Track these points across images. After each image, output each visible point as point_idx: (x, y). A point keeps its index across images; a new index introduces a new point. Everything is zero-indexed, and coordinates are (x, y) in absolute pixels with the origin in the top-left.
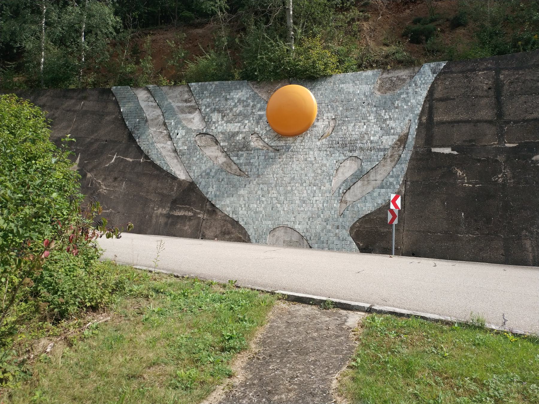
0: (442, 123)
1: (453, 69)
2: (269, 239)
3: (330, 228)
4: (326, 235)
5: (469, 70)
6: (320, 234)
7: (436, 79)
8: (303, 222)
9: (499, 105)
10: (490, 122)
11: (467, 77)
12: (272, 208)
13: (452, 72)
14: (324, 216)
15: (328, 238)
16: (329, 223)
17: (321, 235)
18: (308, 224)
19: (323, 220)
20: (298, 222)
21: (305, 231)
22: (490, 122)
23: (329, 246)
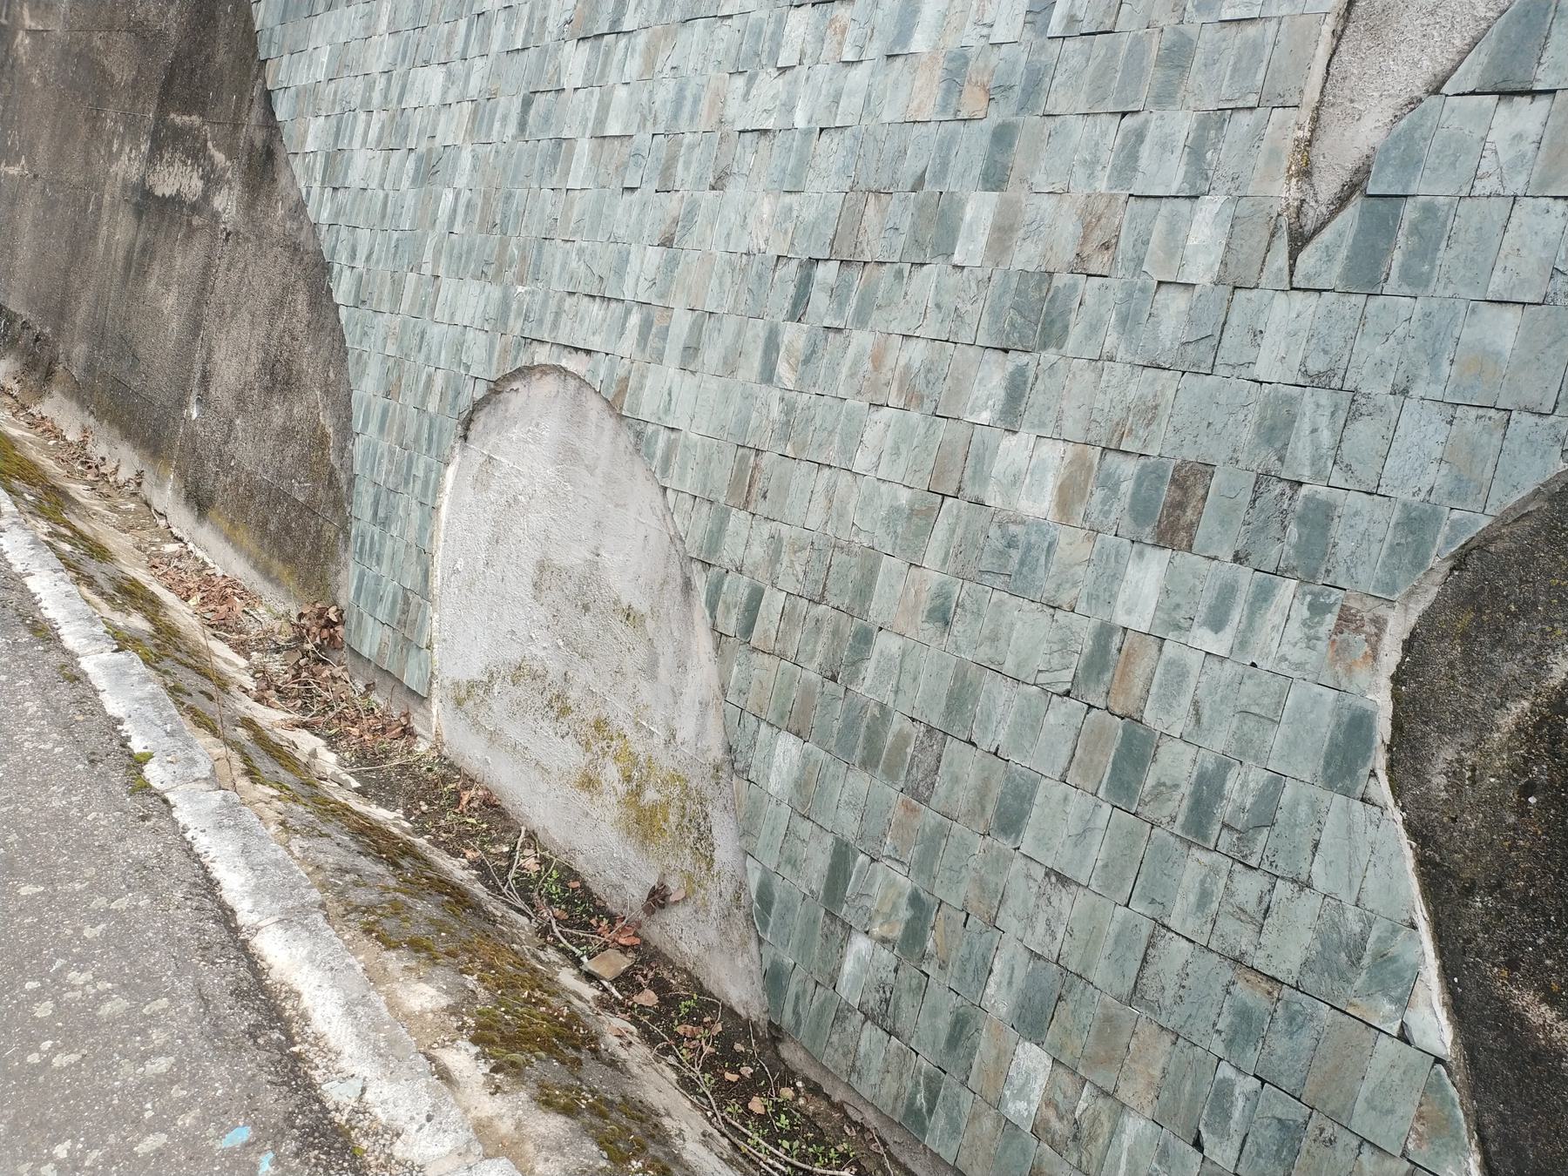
2: (453, 503)
3: (1038, 503)
4: (942, 616)
6: (864, 592)
8: (730, 324)
12: (527, 104)
14: (1003, 234)
15: (960, 698)
16: (1036, 398)
17: (879, 607)
18: (768, 375)
19: (979, 324)
20: (681, 323)
21: (722, 474)
23: (933, 842)
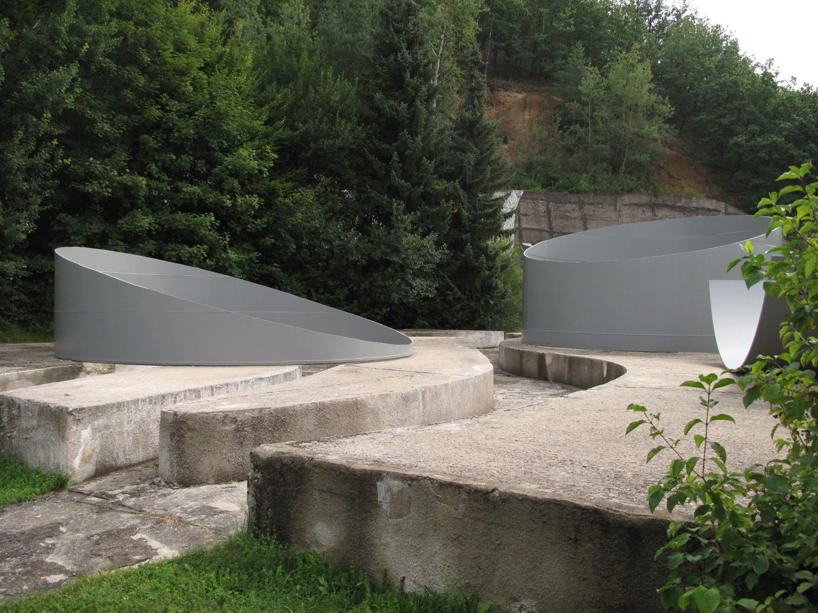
0: (525, 229)
1: (527, 197)
5: (534, 199)
7: (520, 202)
9: (550, 223)
10: (547, 231)
11: (534, 203)
13: (527, 199)
22: (547, 231)
